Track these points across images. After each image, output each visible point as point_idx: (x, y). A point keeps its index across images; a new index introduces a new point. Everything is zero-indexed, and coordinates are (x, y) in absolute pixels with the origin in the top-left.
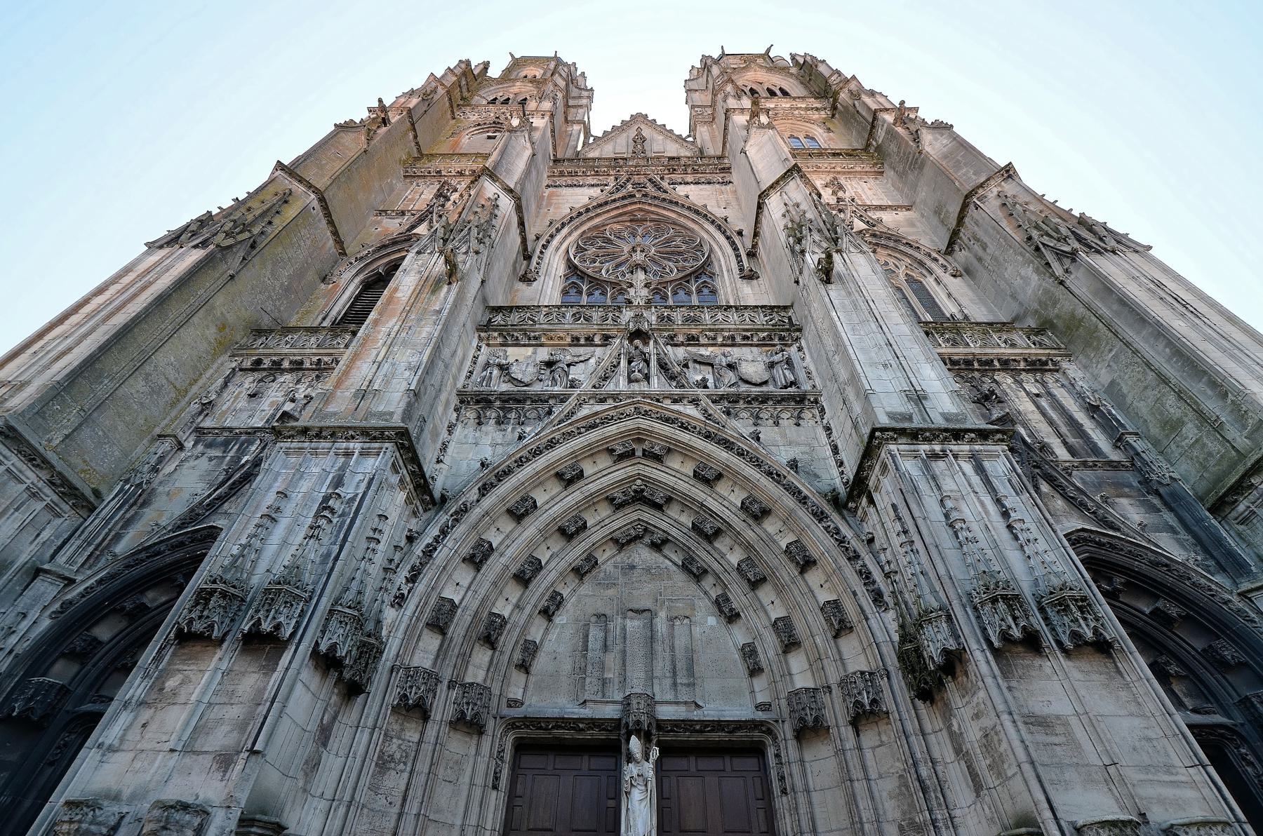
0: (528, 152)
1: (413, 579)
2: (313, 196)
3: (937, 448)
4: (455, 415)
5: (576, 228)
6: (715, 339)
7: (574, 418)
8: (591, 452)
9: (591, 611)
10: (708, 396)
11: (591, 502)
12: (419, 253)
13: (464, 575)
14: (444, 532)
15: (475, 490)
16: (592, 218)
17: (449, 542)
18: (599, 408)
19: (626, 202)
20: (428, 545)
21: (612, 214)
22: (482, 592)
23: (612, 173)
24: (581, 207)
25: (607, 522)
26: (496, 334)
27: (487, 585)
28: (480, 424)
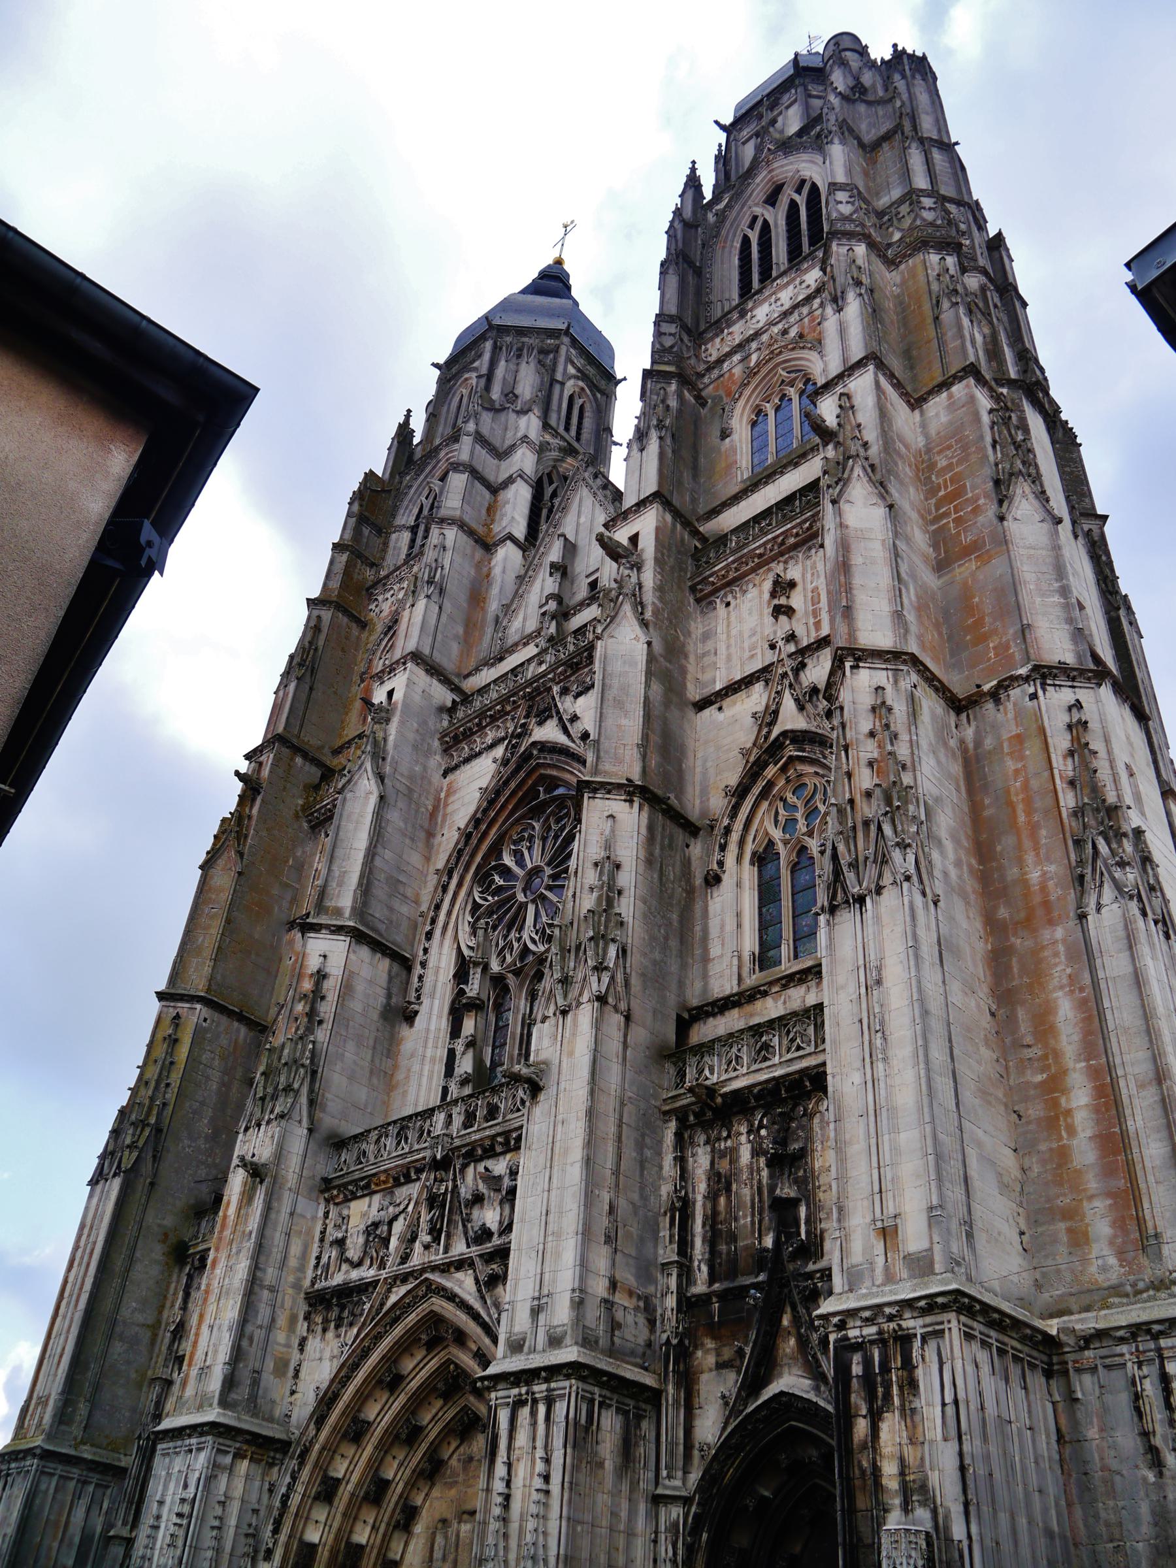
0: (373, 800)
1: (276, 1531)
2: (198, 1006)
3: (524, 1390)
4: (306, 1324)
5: (467, 869)
6: (507, 1142)
7: (384, 1310)
8: (404, 1347)
9: (437, 1517)
10: (481, 1256)
11: (418, 1400)
12: (247, 1129)
13: (320, 1513)
14: (294, 1478)
15: (312, 1426)
16: (485, 834)
17: (300, 1489)
18: (402, 1290)
19: (522, 774)
20: (283, 1495)
21: (501, 821)
22: (336, 1525)
23: (508, 708)
24: (467, 826)
25: (440, 1414)
26: (335, 1192)
27: (339, 1517)
28: (325, 1330)
